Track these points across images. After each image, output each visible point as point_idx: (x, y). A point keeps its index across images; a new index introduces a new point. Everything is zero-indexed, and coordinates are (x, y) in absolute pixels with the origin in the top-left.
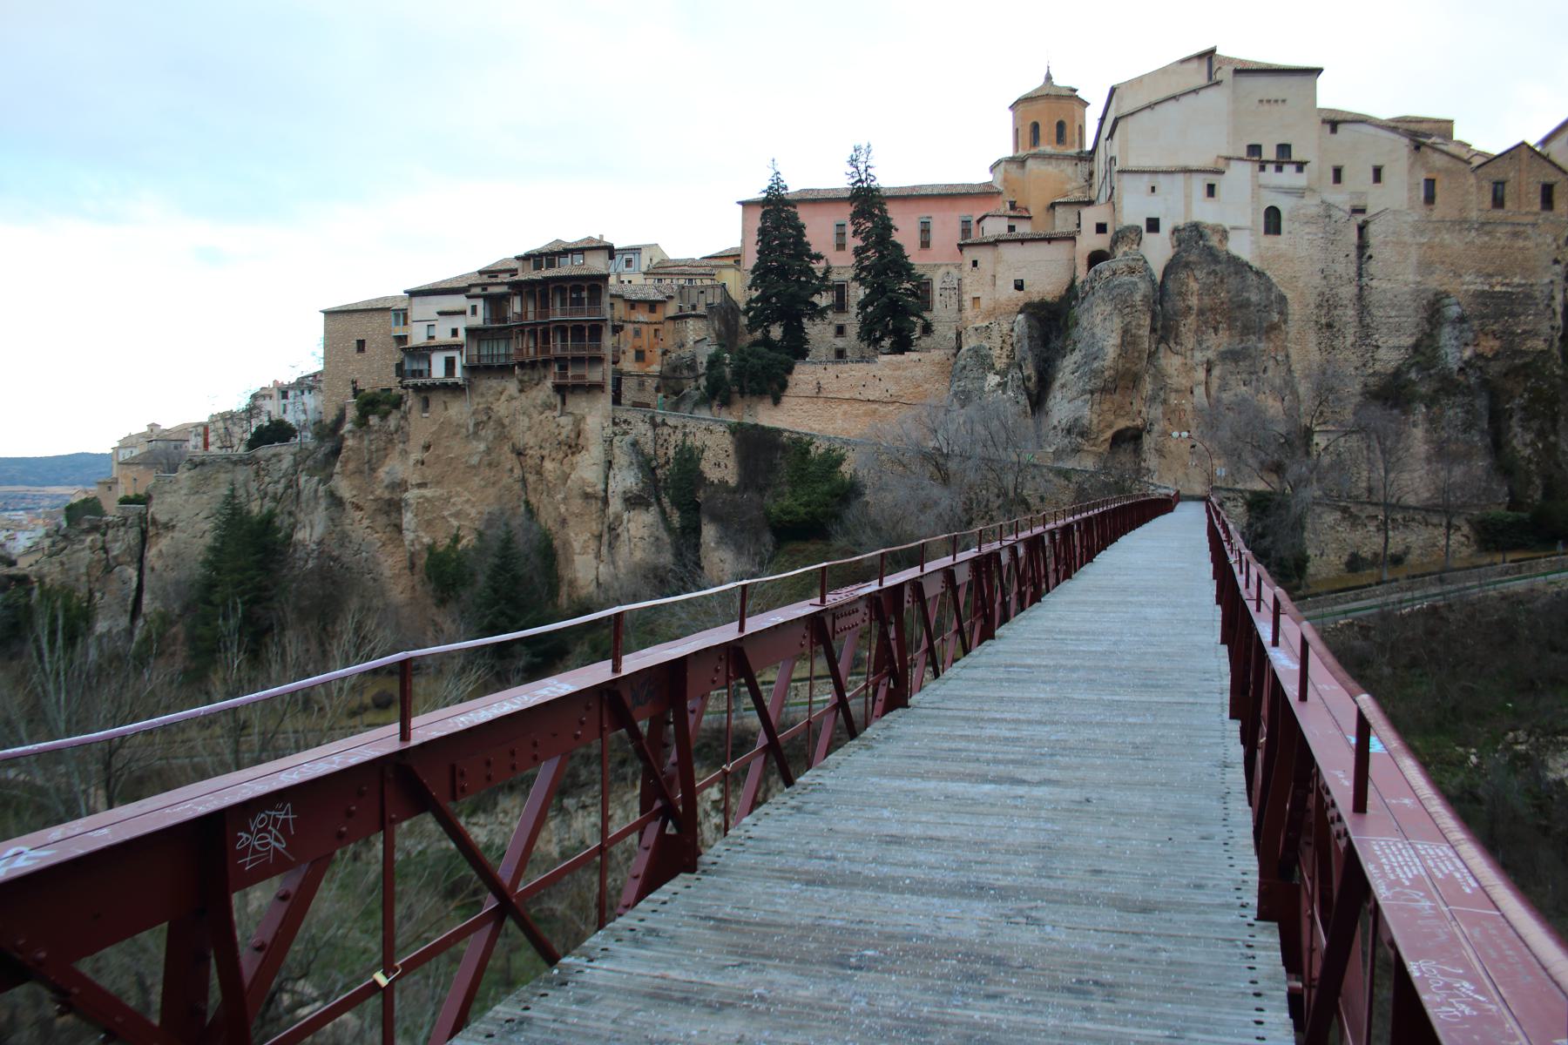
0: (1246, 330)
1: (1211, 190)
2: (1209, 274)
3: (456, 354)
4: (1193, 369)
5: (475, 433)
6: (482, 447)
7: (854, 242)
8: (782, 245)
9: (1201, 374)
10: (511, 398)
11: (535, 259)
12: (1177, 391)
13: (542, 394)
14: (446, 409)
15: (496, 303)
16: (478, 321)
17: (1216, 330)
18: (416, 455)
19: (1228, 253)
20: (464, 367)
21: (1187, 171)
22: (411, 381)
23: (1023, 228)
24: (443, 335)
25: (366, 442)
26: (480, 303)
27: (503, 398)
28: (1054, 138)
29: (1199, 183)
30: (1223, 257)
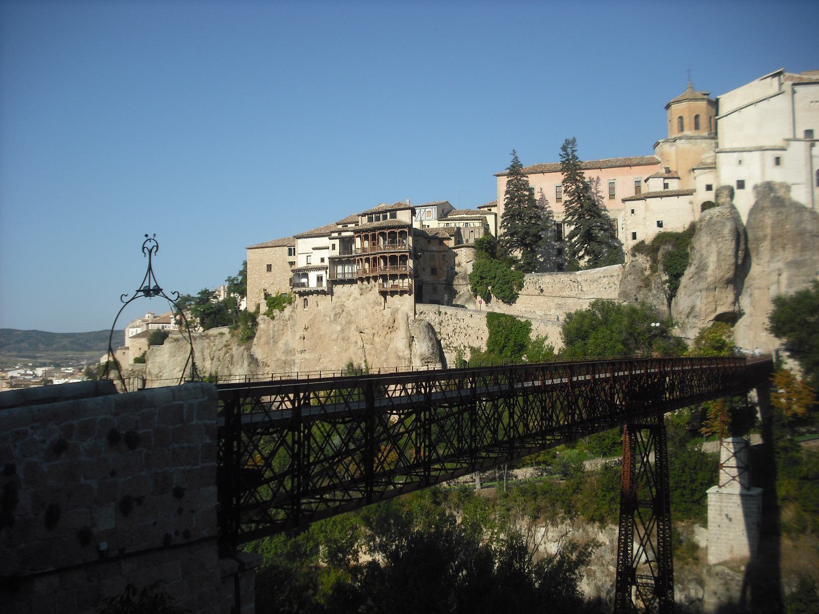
0: (804, 248)
1: (778, 161)
2: (778, 213)
3: (323, 273)
4: (769, 274)
5: (335, 320)
6: (339, 328)
7: (566, 197)
8: (519, 202)
9: (774, 277)
10: (356, 299)
11: (370, 215)
12: (759, 288)
13: (373, 296)
14: (318, 305)
15: (347, 243)
16: (336, 253)
17: (784, 248)
18: (300, 333)
19: (790, 199)
20: (328, 281)
21: (762, 149)
22: (297, 289)
23: (674, 185)
24: (315, 262)
25: (271, 326)
26: (337, 242)
27: (351, 298)
28: (693, 126)
29: (770, 156)
30: (787, 203)
